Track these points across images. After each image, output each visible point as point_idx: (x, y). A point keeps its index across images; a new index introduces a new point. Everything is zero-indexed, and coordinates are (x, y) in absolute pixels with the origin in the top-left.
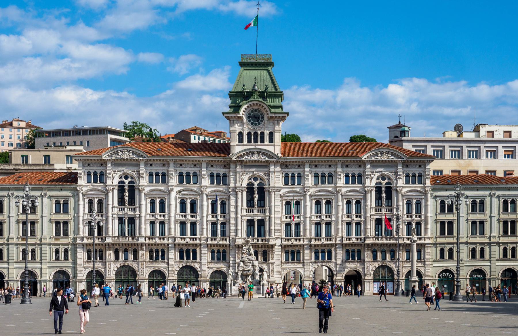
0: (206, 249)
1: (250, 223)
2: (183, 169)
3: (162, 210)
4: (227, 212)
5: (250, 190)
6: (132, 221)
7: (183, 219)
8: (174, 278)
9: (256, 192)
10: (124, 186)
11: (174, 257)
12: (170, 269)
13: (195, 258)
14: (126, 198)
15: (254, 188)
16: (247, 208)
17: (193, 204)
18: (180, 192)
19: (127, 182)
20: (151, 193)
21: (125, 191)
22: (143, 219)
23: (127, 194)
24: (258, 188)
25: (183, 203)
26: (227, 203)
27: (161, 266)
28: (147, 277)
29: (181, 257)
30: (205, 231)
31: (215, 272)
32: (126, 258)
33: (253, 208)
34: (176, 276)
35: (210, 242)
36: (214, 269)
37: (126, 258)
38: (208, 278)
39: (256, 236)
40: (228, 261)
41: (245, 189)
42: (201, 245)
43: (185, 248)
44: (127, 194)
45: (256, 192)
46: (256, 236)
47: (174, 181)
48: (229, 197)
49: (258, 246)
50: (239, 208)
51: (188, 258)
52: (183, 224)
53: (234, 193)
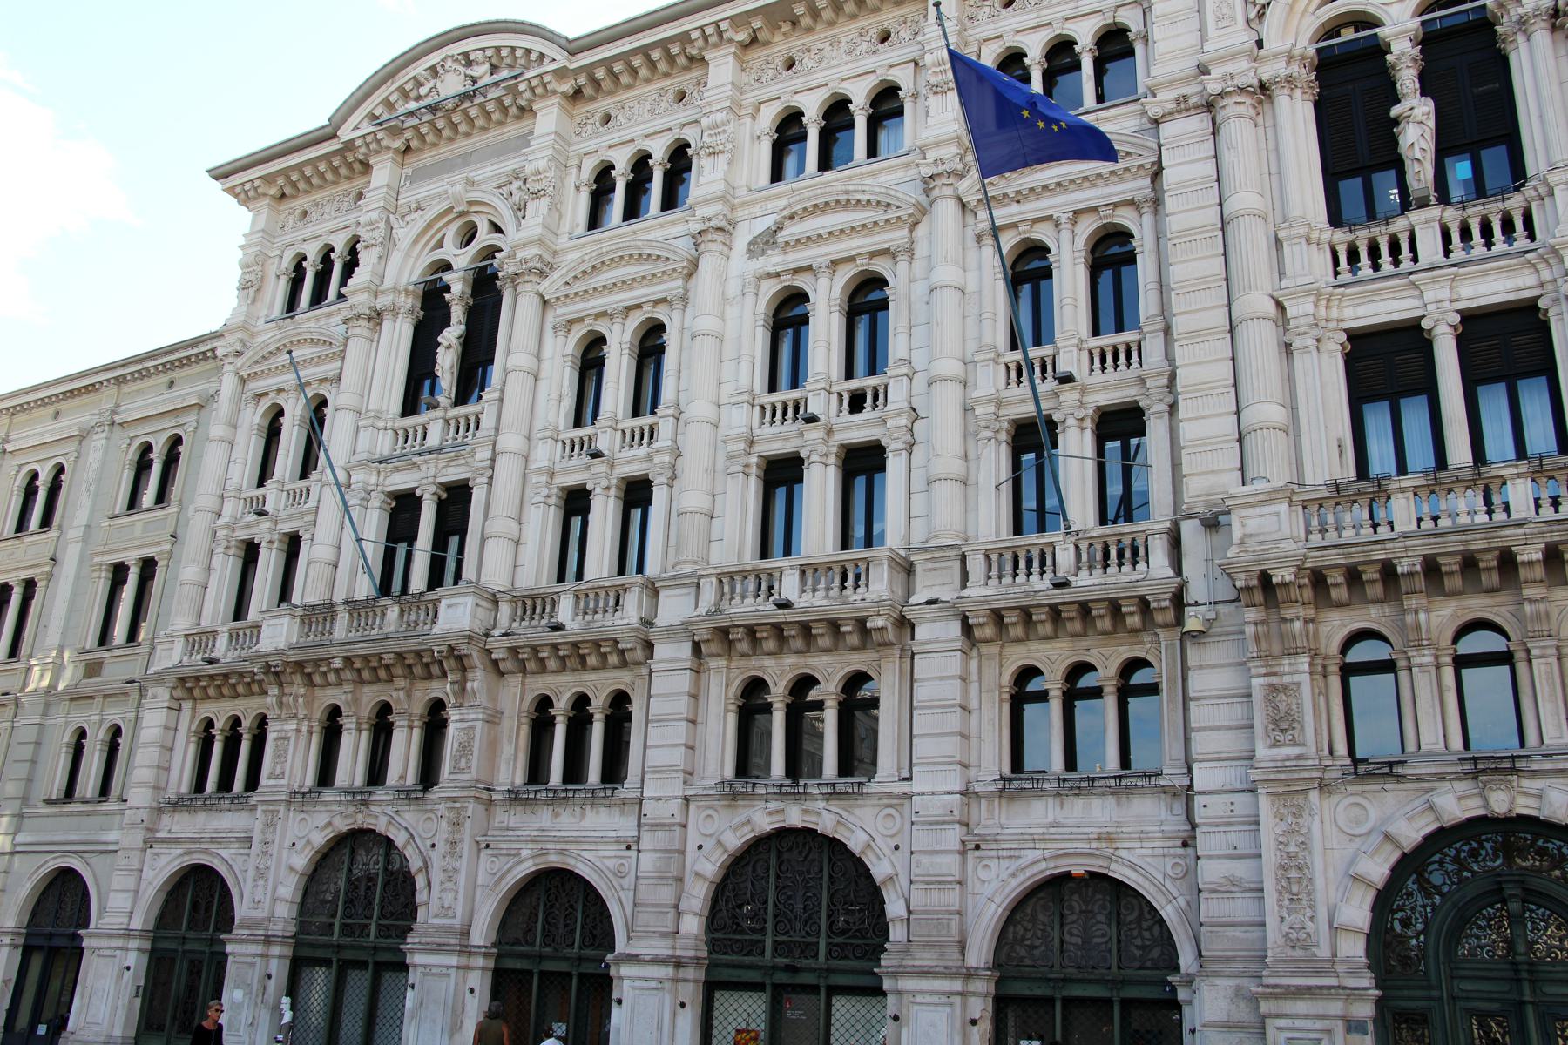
0: (954, 663)
1: (1384, 366)
2: (799, 82)
3: (644, 397)
4: (1147, 304)
5: (1348, 80)
6: (455, 500)
7: (779, 439)
8: (661, 948)
9: (1407, 79)
10: (447, 289)
11: (677, 757)
12: (648, 862)
13: (856, 757)
14: (447, 361)
15: (1379, 50)
16: (1341, 237)
17: (867, 301)
18: (766, 241)
19: (462, 259)
20: (579, 287)
21: (446, 323)
22: (507, 471)
23: (451, 335)
24: (1430, 41)
25: (789, 315)
26: (1142, 230)
27: (585, 837)
28: (482, 934)
29: (747, 761)
30: (946, 495)
31: (1055, 887)
32: (376, 773)
33: (1399, 225)
34: (692, 925)
35: (984, 591)
36: (1036, 865)
37: (376, 773)
38: (979, 954)
39: (1459, 452)
40: (1173, 776)
41: (1306, 76)
42: (905, 624)
43: (779, 673)
44: (451, 335)
45: (1407, 79)
46: (1459, 452)
47: (732, 169)
48: (1157, 173)
49: (1507, 561)
50: (1252, 241)
51: (799, 763)
52: (782, 474)
53: (1199, 123)
